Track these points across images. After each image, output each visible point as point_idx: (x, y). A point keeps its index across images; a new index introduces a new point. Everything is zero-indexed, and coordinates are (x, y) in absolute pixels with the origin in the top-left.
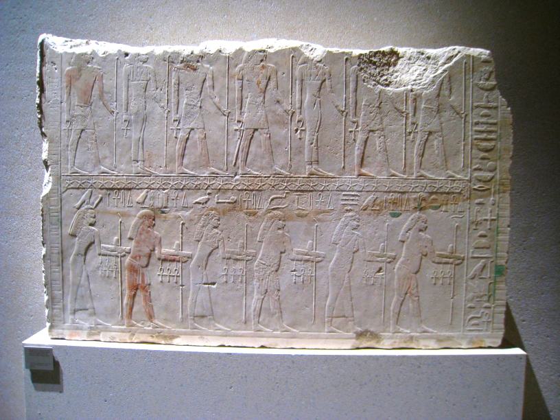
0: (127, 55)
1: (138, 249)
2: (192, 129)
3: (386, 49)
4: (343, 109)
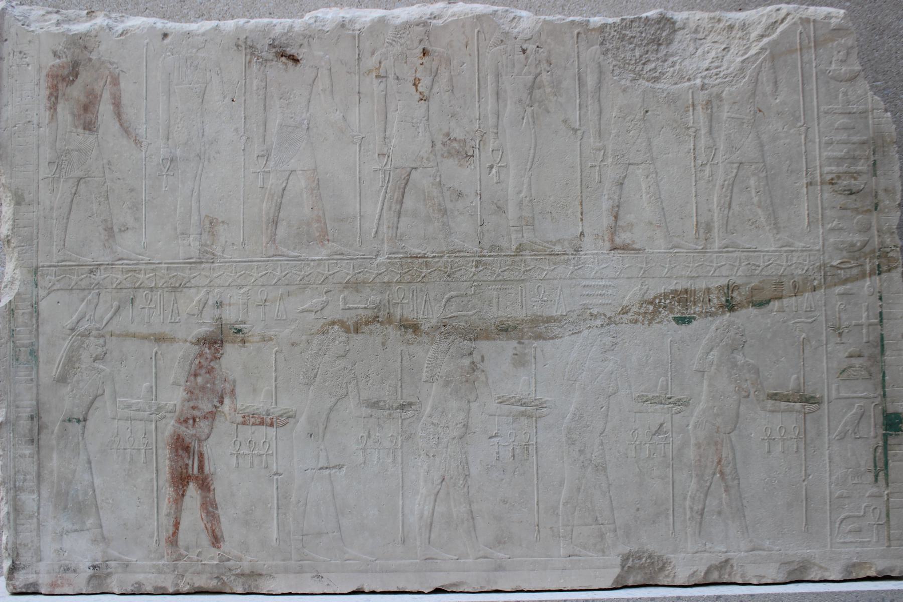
0: (165, 35)
1: (191, 404)
2: (292, 171)
3: (652, 13)
4: (577, 125)
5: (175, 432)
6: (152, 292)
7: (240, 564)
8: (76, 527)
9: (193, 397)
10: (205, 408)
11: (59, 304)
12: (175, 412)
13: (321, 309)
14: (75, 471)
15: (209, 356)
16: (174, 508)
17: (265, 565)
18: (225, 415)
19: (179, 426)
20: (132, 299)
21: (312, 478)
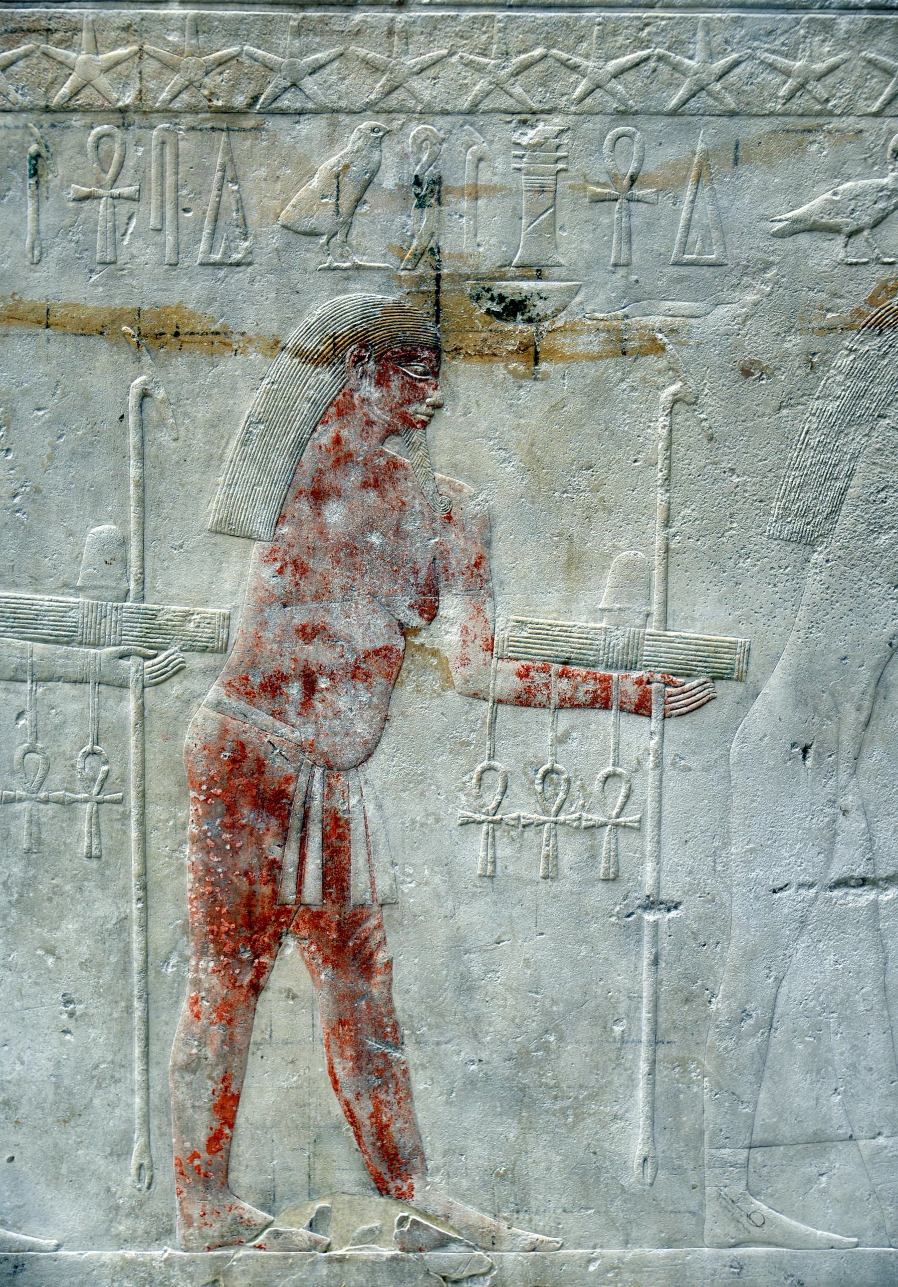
1: (299, 616)
6: (125, 126)
7: (488, 1258)
9: (308, 587)
10: (358, 634)
12: (224, 650)
13: (876, 225)
15: (380, 415)
16: (217, 1041)
17: (590, 1261)
18: (443, 665)
19: (243, 705)
20: (37, 156)
21: (803, 923)
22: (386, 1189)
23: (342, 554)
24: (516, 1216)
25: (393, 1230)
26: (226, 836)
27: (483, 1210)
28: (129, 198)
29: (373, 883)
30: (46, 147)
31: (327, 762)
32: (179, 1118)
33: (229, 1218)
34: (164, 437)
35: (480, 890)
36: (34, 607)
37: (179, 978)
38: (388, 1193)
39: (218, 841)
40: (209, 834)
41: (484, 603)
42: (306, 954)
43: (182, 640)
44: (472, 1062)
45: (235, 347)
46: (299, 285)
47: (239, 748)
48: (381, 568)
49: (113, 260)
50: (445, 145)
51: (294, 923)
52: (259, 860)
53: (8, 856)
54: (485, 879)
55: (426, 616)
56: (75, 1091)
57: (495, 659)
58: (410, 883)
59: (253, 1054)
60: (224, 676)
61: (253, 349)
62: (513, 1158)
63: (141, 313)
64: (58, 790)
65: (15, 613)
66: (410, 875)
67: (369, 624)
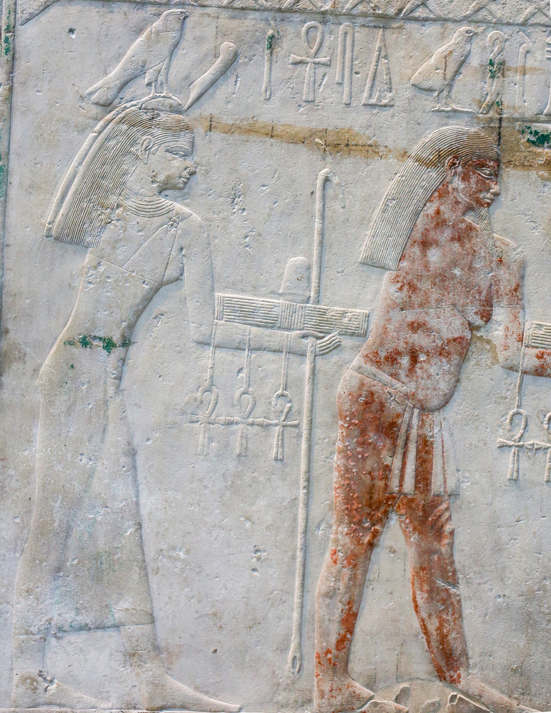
1: (410, 316)
5: (362, 384)
6: (324, 22)
8: (82, 619)
9: (416, 299)
11: (74, 36)
12: (365, 335)
14: (91, 474)
15: (463, 198)
16: (346, 579)
18: (493, 350)
19: (374, 369)
20: (272, 37)
22: (444, 677)
23: (437, 280)
24: (522, 697)
25: (447, 703)
26: (359, 449)
27: (503, 692)
28: (324, 64)
29: (445, 482)
30: (278, 32)
31: (422, 406)
32: (320, 627)
33: (347, 693)
34: (337, 206)
35: (508, 488)
36: (253, 305)
37: (326, 539)
38: (445, 679)
39: (354, 452)
40: (349, 448)
41: (519, 313)
42: (403, 525)
43: (340, 328)
44: (499, 596)
45: (381, 154)
46: (420, 120)
47: (370, 395)
48: (459, 289)
49: (312, 100)
50: (508, 43)
51: (397, 505)
52: (378, 465)
53: (226, 458)
54: (512, 481)
55: (485, 319)
56: (257, 608)
57: (524, 347)
58: (467, 482)
59: (367, 587)
60: (364, 350)
61: (391, 156)
62: (522, 659)
63: (327, 131)
64: (260, 418)
65: (241, 308)
66: (468, 477)
67: (451, 322)
